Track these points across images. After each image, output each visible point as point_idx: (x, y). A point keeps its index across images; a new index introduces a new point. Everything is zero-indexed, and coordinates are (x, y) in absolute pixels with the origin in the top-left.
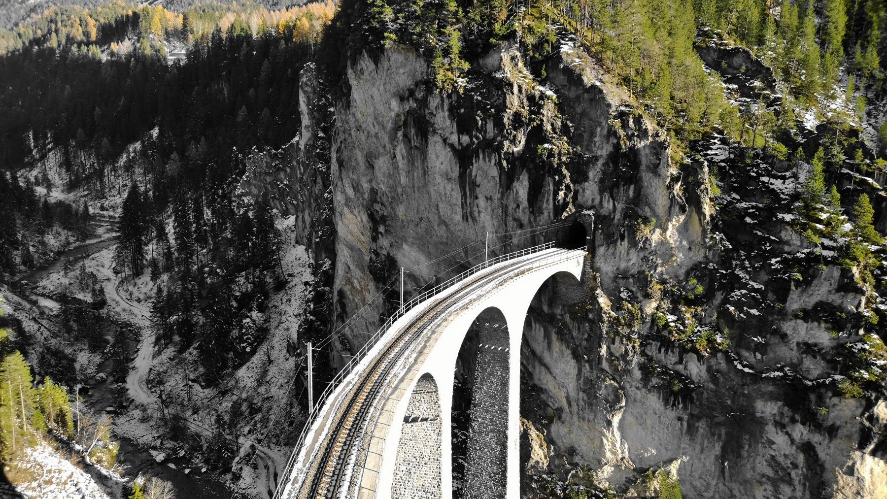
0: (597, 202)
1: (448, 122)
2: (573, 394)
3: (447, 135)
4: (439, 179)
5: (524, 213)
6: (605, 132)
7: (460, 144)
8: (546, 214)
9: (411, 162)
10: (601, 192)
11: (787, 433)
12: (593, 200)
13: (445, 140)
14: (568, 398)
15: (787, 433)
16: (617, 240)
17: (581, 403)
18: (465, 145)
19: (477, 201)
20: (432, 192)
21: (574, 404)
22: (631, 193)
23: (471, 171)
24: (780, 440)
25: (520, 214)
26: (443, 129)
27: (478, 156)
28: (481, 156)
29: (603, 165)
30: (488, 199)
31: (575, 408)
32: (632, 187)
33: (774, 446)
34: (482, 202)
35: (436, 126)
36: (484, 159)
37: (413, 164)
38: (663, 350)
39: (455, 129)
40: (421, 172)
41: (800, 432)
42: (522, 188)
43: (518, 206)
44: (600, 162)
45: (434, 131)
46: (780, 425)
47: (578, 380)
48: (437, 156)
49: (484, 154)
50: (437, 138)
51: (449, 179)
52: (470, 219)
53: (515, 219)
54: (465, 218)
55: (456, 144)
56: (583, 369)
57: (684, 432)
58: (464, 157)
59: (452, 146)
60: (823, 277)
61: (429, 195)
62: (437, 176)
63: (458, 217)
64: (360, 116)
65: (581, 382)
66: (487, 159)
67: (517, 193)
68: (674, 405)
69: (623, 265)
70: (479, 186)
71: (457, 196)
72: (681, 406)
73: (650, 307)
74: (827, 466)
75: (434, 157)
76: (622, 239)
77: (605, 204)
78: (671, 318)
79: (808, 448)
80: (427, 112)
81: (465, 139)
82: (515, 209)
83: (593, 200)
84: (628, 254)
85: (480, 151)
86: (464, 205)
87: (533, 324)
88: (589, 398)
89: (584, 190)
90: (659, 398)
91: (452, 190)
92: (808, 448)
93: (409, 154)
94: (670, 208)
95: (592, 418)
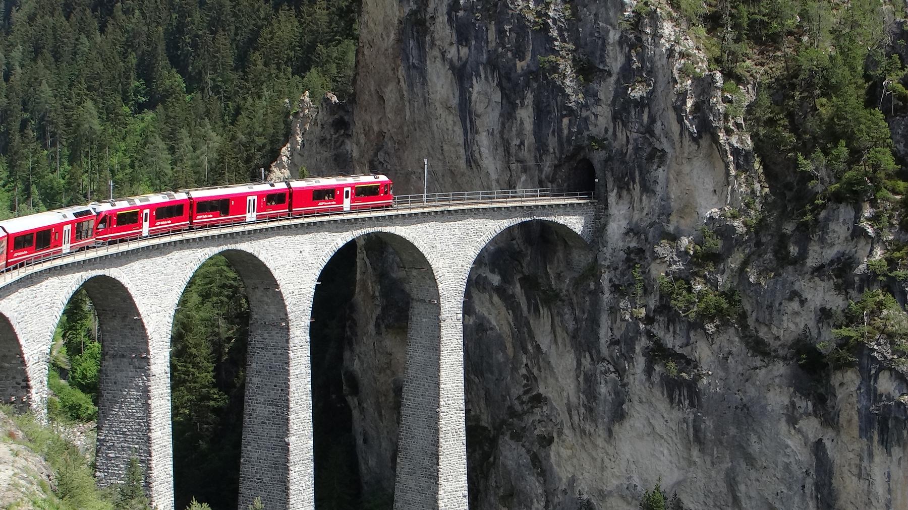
0: (611, 130)
1: (448, 30)
2: (574, 400)
3: (446, 47)
4: (440, 111)
5: (529, 151)
6: (617, 37)
7: (460, 59)
8: (552, 150)
9: (411, 86)
10: (614, 118)
11: (799, 431)
12: (606, 130)
13: (443, 54)
14: (568, 405)
15: (799, 431)
16: (628, 184)
17: (582, 410)
18: (464, 59)
19: (477, 137)
20: (435, 128)
21: (574, 412)
22: (645, 117)
23: (471, 93)
24: (794, 443)
25: (525, 154)
26: (442, 40)
27: (478, 75)
28: (483, 76)
29: (618, 81)
30: (491, 134)
31: (576, 418)
32: (646, 110)
33: (788, 450)
34: (483, 140)
35: (436, 36)
36: (486, 77)
37: (412, 90)
38: (671, 329)
39: (455, 38)
40: (422, 99)
41: (811, 427)
42: (526, 115)
43: (522, 143)
44: (612, 80)
45: (433, 44)
46: (792, 421)
47: (578, 377)
48: (438, 77)
49: (485, 69)
50: (436, 52)
51: (449, 108)
52: (473, 165)
53: (519, 161)
54: (468, 162)
55: (455, 59)
56: (583, 360)
57: (691, 436)
58: (462, 75)
59: (451, 60)
60: (841, 220)
61: (433, 134)
62: (438, 105)
63: (462, 164)
64: (372, 25)
65: (581, 379)
66: (490, 79)
67: (522, 123)
68: (680, 401)
69: (637, 216)
70: (479, 116)
71: (459, 131)
72: (687, 402)
73: (137, 83)
74: (836, 469)
75: (435, 79)
76: (634, 183)
77: (619, 134)
78: (282, 139)
79: (818, 447)
80: (428, 17)
81: (464, 51)
82: (519, 146)
83: (606, 130)
84: (641, 200)
85: (481, 67)
86: (467, 145)
87: (541, 308)
88: (588, 401)
89: (596, 116)
90: (663, 393)
91: (455, 123)
92: (818, 447)
93: (409, 76)
94: (681, 134)
95: (592, 431)
